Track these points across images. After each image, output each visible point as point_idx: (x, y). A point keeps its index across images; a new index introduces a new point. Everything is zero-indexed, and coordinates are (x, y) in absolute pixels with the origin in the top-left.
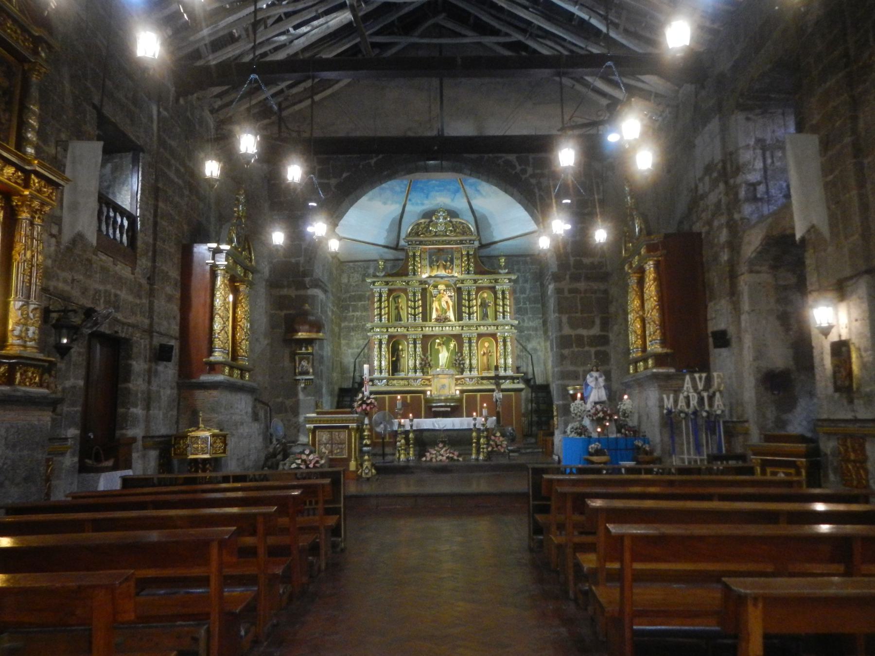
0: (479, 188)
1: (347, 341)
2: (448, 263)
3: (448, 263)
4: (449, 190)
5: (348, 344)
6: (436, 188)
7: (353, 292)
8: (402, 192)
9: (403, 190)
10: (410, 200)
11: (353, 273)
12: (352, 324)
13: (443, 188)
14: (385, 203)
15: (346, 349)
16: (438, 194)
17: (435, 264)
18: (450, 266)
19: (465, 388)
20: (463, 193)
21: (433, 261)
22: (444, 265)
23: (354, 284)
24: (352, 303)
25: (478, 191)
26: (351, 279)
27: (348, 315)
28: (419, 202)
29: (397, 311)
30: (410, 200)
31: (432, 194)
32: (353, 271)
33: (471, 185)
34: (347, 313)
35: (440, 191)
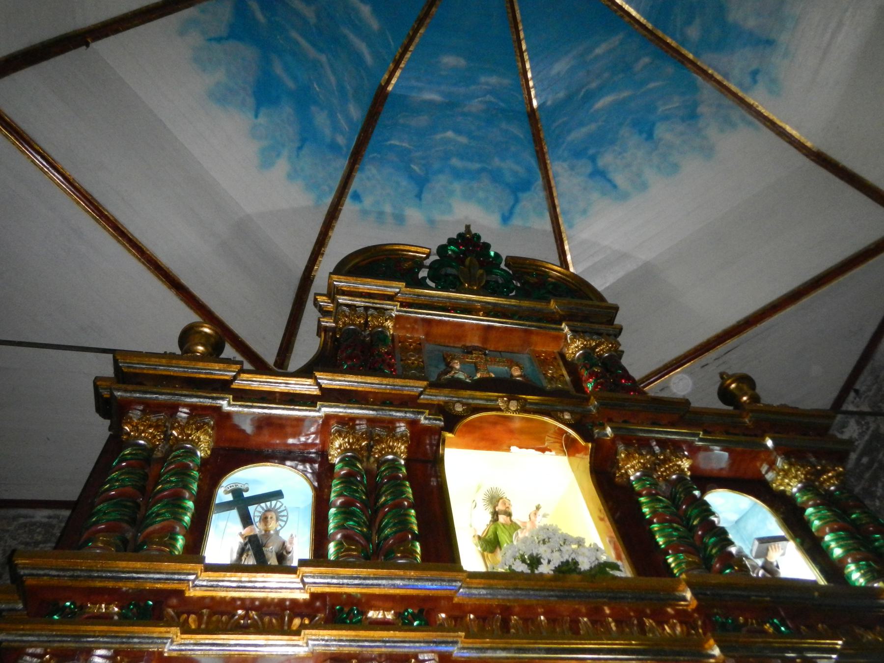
0: (606, 160)
4: (496, 177)
6: (455, 162)
8: (334, 147)
9: (341, 140)
10: (357, 197)
13: (478, 166)
14: (267, 160)
16: (457, 186)
25: (599, 174)
28: (388, 208)
30: (357, 197)
31: (440, 182)
32: (39, 538)
33: (578, 153)
35: (475, 175)
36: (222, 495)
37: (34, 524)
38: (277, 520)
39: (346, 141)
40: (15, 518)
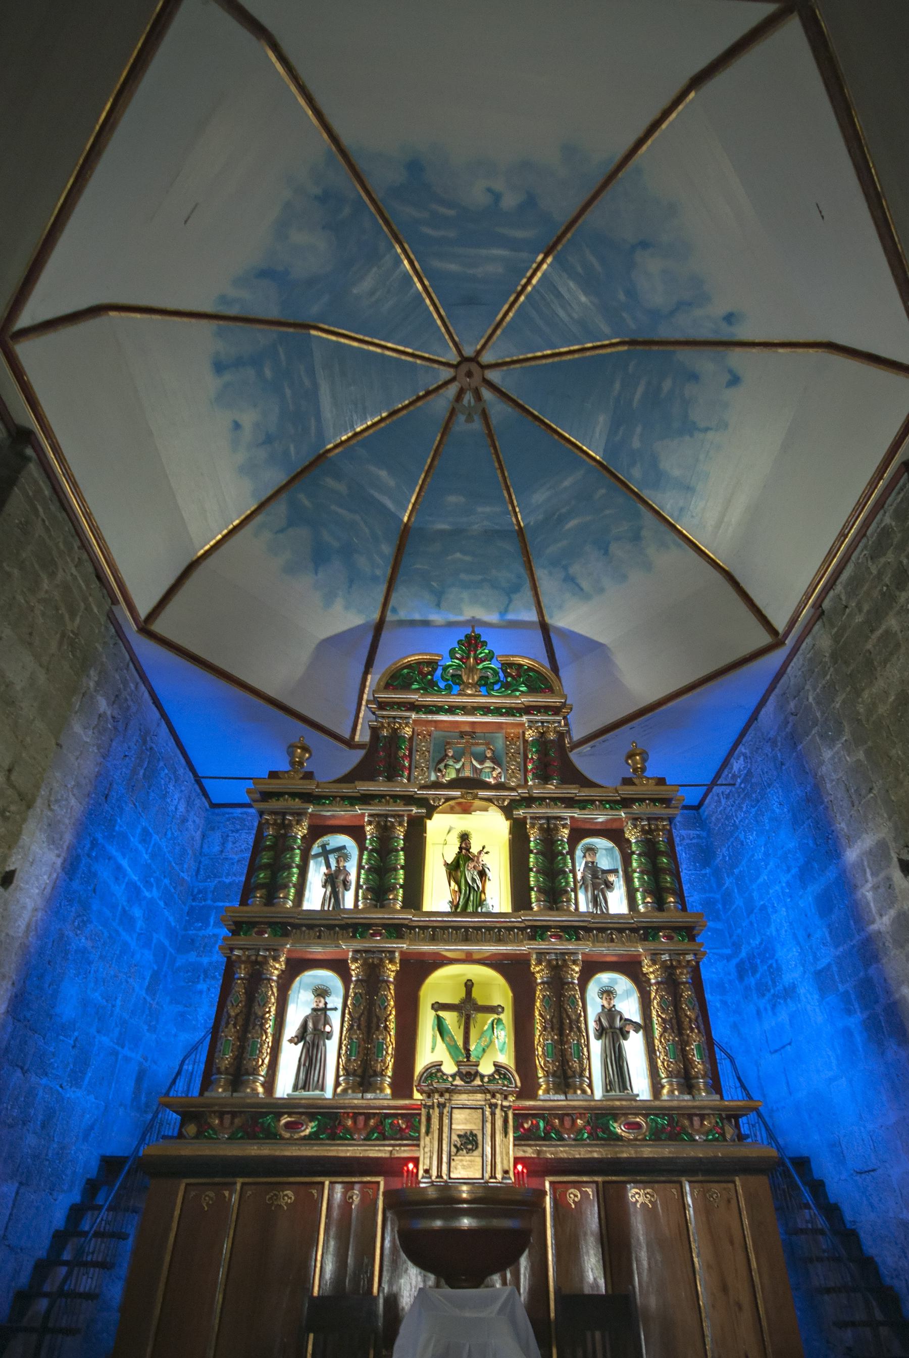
1: (180, 1008)
2: (488, 764)
3: (488, 764)
5: (182, 1015)
7: (228, 875)
11: (237, 831)
12: (205, 960)
15: (174, 1031)
17: (451, 763)
18: (494, 769)
19: (550, 1152)
20: (528, 594)
21: (446, 755)
22: (473, 765)
23: (236, 858)
24: (221, 904)
26: (230, 845)
27: (201, 933)
29: (329, 889)
32: (238, 827)
34: (200, 929)
36: (316, 849)
37: (234, 818)
38: (345, 861)
39: (383, 571)
40: (224, 814)
